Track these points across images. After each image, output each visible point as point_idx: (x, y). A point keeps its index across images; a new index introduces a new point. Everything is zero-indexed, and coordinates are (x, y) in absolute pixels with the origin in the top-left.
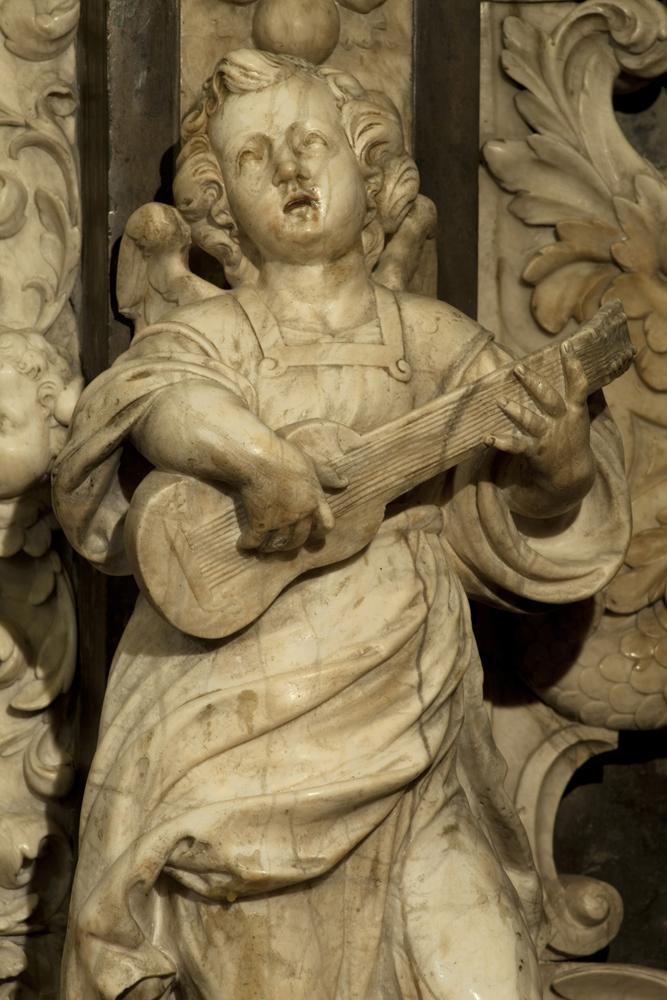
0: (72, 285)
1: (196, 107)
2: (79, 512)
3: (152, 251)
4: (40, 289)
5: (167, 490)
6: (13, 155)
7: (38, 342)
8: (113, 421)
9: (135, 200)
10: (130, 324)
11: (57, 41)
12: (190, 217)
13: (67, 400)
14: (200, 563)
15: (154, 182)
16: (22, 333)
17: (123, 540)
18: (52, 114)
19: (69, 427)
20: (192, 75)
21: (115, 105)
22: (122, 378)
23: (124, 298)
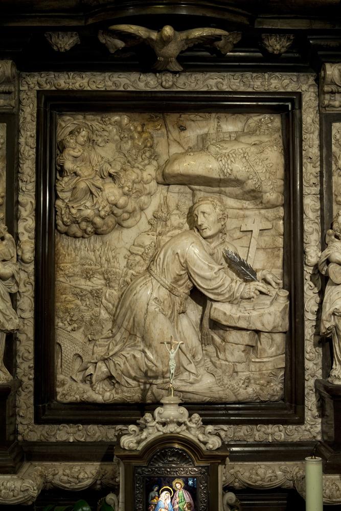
0: (320, 240)
1: (335, 218)
2: (322, 268)
3: (330, 235)
4: (316, 241)
5: (332, 265)
6: (312, 224)
7: (316, 247)
8: (325, 257)
9: (328, 229)
10: (327, 245)
11: (318, 210)
12: (335, 231)
13: (320, 254)
14: (337, 274)
15: (330, 227)
16: (314, 246)
17: (327, 271)
18: (317, 219)
19: (320, 258)
20: (335, 214)
21: (325, 217)
22: (326, 251)
23: (326, 241)
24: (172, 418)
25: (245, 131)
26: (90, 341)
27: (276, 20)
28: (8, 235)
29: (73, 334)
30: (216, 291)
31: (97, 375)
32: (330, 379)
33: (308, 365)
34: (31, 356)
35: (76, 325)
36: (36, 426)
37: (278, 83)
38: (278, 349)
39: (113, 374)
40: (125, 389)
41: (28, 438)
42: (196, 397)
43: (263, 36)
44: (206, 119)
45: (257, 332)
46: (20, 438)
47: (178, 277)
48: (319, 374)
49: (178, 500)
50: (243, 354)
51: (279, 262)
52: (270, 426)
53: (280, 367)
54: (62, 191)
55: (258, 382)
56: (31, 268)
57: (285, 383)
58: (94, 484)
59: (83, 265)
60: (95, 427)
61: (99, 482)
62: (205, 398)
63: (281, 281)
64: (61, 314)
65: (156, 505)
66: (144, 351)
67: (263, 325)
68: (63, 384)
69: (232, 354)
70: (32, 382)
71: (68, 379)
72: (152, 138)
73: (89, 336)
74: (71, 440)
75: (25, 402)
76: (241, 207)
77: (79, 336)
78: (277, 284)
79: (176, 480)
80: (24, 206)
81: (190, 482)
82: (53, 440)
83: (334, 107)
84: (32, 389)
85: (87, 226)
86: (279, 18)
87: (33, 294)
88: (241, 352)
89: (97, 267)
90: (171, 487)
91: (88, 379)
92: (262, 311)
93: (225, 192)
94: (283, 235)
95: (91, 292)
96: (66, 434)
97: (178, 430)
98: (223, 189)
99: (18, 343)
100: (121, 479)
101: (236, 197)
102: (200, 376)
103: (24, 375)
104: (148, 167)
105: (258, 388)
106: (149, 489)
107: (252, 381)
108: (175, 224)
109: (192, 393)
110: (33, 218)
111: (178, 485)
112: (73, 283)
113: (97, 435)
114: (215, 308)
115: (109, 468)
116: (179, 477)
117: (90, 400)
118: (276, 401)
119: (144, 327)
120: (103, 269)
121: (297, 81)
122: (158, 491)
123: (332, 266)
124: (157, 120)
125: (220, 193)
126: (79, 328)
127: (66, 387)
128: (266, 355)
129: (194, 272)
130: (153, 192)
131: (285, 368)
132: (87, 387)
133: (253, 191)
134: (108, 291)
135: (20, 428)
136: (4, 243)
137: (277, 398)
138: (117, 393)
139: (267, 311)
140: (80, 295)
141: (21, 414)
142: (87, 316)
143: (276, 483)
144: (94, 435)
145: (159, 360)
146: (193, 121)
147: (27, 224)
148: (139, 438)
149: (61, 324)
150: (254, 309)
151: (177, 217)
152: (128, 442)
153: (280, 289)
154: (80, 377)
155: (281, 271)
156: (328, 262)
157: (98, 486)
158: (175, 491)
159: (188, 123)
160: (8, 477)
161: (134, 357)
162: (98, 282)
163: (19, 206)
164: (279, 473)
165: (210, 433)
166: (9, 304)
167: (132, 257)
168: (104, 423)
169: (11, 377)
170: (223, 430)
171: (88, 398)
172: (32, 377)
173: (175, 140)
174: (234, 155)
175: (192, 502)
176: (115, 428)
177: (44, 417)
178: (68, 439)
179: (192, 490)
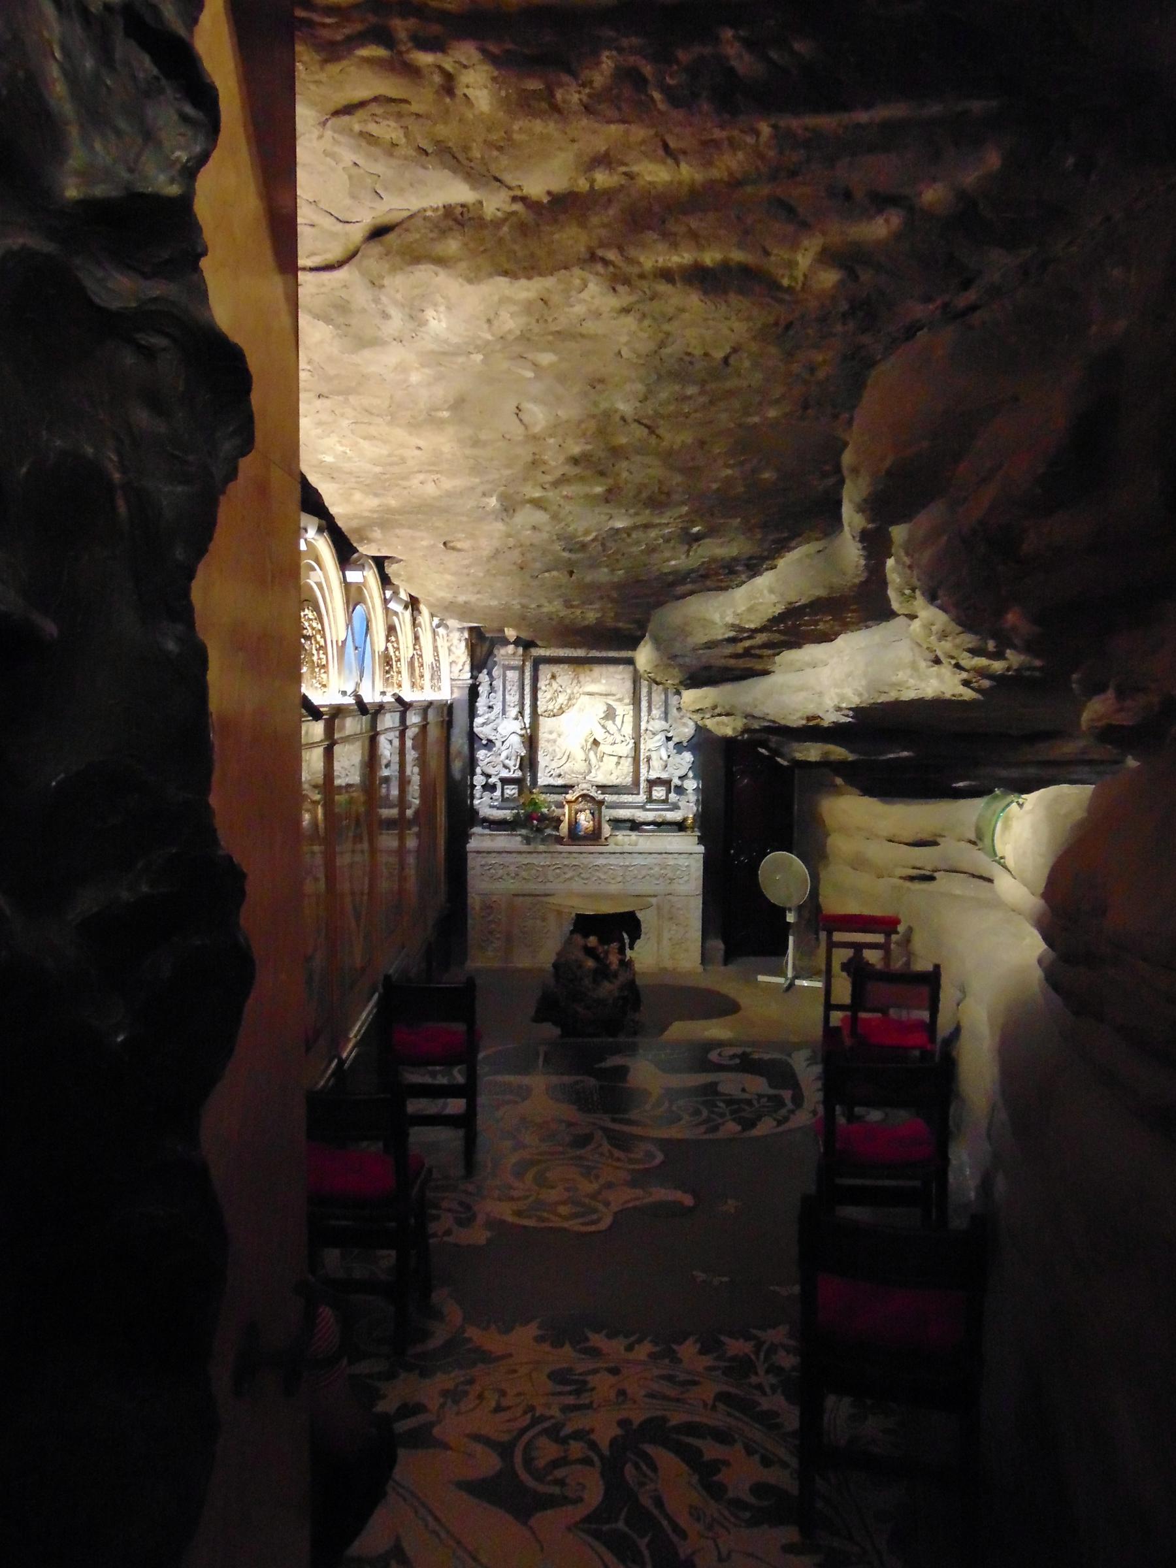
28: (520, 718)
33: (642, 771)
45: (621, 757)
101: (614, 700)
140: (548, 741)
142: (550, 749)
143: (626, 818)
147: (527, 711)
152: (569, 797)
168: (559, 794)
179: (593, 814)
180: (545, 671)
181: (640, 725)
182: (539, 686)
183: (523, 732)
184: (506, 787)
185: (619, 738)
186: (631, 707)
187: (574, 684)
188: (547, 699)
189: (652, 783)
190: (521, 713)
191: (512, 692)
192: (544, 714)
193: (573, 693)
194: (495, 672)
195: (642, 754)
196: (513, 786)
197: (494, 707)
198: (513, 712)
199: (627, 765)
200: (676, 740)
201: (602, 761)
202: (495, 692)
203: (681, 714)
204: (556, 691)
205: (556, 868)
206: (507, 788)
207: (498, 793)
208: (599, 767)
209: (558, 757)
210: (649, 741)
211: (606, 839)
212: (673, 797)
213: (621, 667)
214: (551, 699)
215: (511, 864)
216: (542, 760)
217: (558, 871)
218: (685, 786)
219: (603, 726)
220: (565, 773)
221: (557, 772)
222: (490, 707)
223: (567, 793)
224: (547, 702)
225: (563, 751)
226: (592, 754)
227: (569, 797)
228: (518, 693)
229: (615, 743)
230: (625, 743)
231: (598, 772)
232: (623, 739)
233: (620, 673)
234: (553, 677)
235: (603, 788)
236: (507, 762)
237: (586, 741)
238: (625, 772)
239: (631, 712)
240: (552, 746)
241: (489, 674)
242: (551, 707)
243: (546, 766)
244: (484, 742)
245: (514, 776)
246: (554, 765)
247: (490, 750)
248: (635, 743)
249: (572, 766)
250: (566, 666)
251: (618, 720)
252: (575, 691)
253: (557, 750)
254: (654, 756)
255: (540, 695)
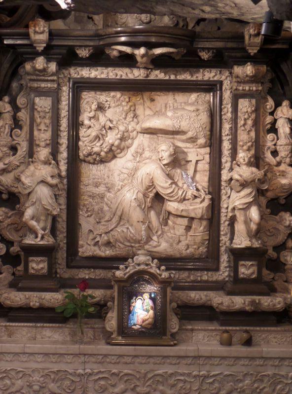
22: (231, 174)
24: (143, 261)
25: (189, 102)
26: (97, 222)
27: (206, 43)
28: (53, 162)
29: (88, 219)
30: (170, 195)
31: (102, 242)
32: (232, 245)
34: (65, 230)
35: (90, 213)
36: (67, 269)
37: (209, 75)
38: (204, 228)
39: (112, 241)
40: (117, 249)
41: (62, 276)
42: (157, 254)
43: (199, 50)
44: (167, 95)
45: (192, 219)
46: (58, 276)
47: (148, 187)
48: (228, 244)
49: (146, 304)
50: (184, 231)
51: (206, 179)
52: (199, 272)
53: (205, 238)
54: (83, 137)
55: (193, 247)
56: (65, 181)
57: (208, 248)
58: (101, 300)
59: (94, 179)
60: (101, 271)
61: (103, 299)
62: (163, 255)
63: (207, 190)
64: (81, 207)
65: (134, 307)
66: (128, 228)
67: (196, 214)
68: (83, 247)
69: (179, 231)
70: (65, 245)
71: (85, 243)
72: (135, 105)
73: (97, 220)
74: (87, 278)
75: (61, 256)
76: (185, 146)
77: (91, 219)
78: (205, 192)
79: (145, 294)
80: (61, 145)
81: (153, 296)
82: (77, 277)
83: (239, 90)
84: (65, 249)
85: (97, 157)
86: (207, 41)
87: (66, 196)
88: (183, 230)
89: (103, 180)
90: (143, 297)
91: (96, 244)
92: (195, 207)
93: (176, 138)
94: (210, 163)
95: (98, 195)
96: (84, 274)
97: (146, 268)
98: (175, 136)
99: (57, 223)
100: (116, 294)
101: (183, 141)
102: (160, 243)
103: (61, 241)
104: (132, 123)
105: (193, 250)
106: (130, 298)
107: (190, 246)
108: (147, 156)
109: (155, 252)
110: (67, 152)
111: (146, 296)
112: (87, 190)
113: (102, 275)
114: (169, 205)
115: (109, 292)
116: (147, 292)
117: (98, 255)
118: (204, 258)
119: (129, 214)
120: (105, 182)
121: (220, 74)
122: (135, 299)
123: (233, 182)
124: (138, 95)
125: (173, 138)
126: (91, 215)
127: (84, 248)
128: (198, 232)
129: (158, 185)
130: (135, 137)
131: (209, 240)
132: (96, 248)
133: (192, 138)
134: (108, 194)
135: (58, 271)
136: (51, 166)
137: (204, 256)
138: (113, 252)
139: (198, 206)
140: (93, 196)
141: (59, 262)
142: (96, 208)
143: (201, 302)
144: (100, 275)
145: (137, 234)
146: (159, 96)
147: (64, 155)
148: (125, 272)
149: (81, 213)
150: (191, 206)
151: (149, 152)
152: (119, 274)
153: (206, 194)
154: (93, 243)
155: (208, 184)
156: (231, 179)
157: (103, 302)
158: (144, 300)
159: (156, 97)
160: (55, 293)
161: (123, 231)
162: (102, 189)
163: (59, 146)
164: (203, 297)
165: (163, 270)
166: (54, 200)
167: (122, 175)
169: (55, 241)
170: (172, 273)
171: (97, 254)
172: (65, 242)
173: (148, 107)
174: (181, 117)
175: (153, 306)
176: (111, 271)
177: (72, 264)
178: (85, 277)
180: (90, 100)
181: (220, 175)
182: (81, 119)
183: (54, 181)
184: (31, 258)
185: (189, 195)
186: (208, 150)
187: (129, 118)
188: (91, 137)
189: (238, 255)
190: (55, 154)
191: (42, 127)
192: (87, 159)
193: (127, 131)
194: (21, 101)
195: (222, 215)
196: (39, 259)
197: (19, 148)
198: (43, 153)
199: (200, 231)
200: (270, 195)
201: (166, 224)
202: (20, 128)
203: (278, 159)
204: (104, 127)
205: (100, 379)
206: (33, 260)
207: (21, 268)
208: (163, 233)
209: (106, 219)
210: (234, 195)
211: (173, 335)
212: (267, 274)
213: (194, 96)
214: (97, 138)
215: (33, 371)
216: (86, 223)
217: (102, 382)
218: (282, 260)
219: (169, 176)
220: (116, 240)
221: (105, 238)
222: (14, 149)
223: (118, 268)
224: (91, 142)
225: (114, 210)
226: (152, 214)
227: (119, 274)
228: (50, 129)
229: (184, 199)
230: (198, 200)
231: (161, 240)
232: (195, 193)
233: (192, 104)
234: (101, 108)
235: (167, 261)
236: (34, 223)
237: (145, 196)
238: (198, 239)
239: (208, 156)
240: (97, 203)
241: (13, 103)
242: (96, 149)
243: (91, 231)
244: (5, 196)
245: (41, 243)
246: (101, 228)
247: (13, 209)
248: (212, 199)
249: (125, 230)
250: (118, 94)
251: (191, 168)
252: (130, 128)
253: (106, 208)
254: (240, 217)
255: (82, 132)
